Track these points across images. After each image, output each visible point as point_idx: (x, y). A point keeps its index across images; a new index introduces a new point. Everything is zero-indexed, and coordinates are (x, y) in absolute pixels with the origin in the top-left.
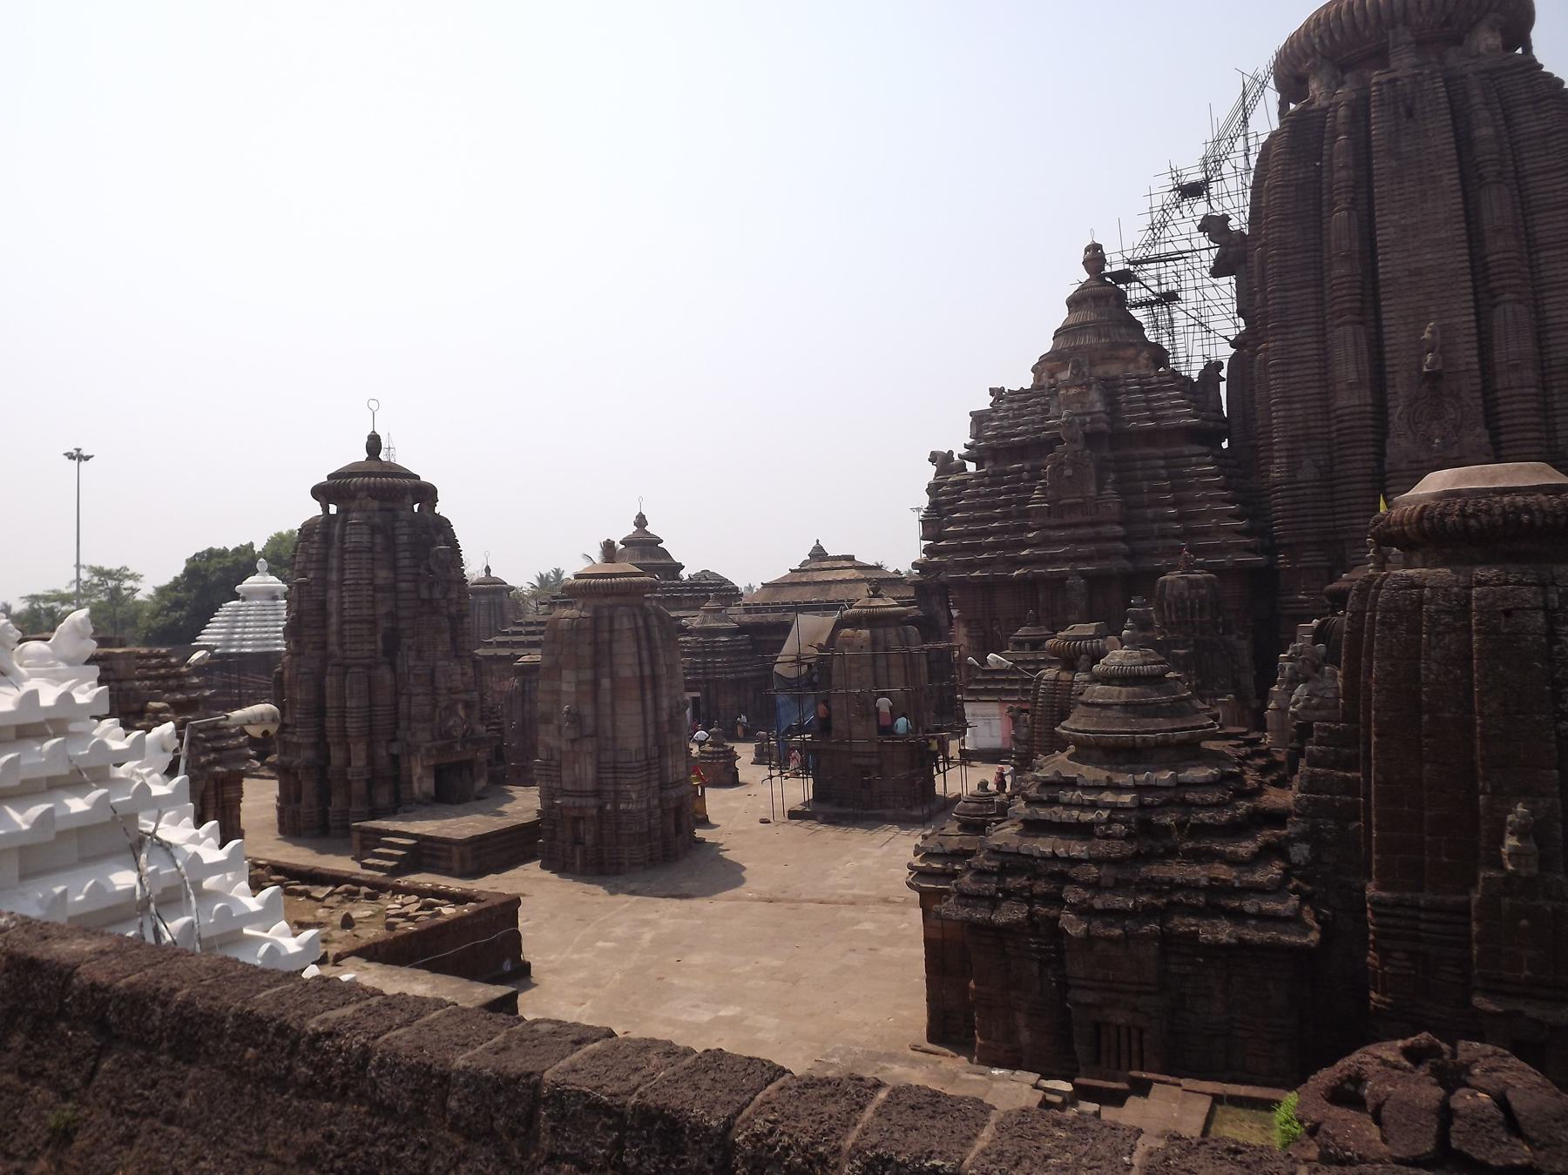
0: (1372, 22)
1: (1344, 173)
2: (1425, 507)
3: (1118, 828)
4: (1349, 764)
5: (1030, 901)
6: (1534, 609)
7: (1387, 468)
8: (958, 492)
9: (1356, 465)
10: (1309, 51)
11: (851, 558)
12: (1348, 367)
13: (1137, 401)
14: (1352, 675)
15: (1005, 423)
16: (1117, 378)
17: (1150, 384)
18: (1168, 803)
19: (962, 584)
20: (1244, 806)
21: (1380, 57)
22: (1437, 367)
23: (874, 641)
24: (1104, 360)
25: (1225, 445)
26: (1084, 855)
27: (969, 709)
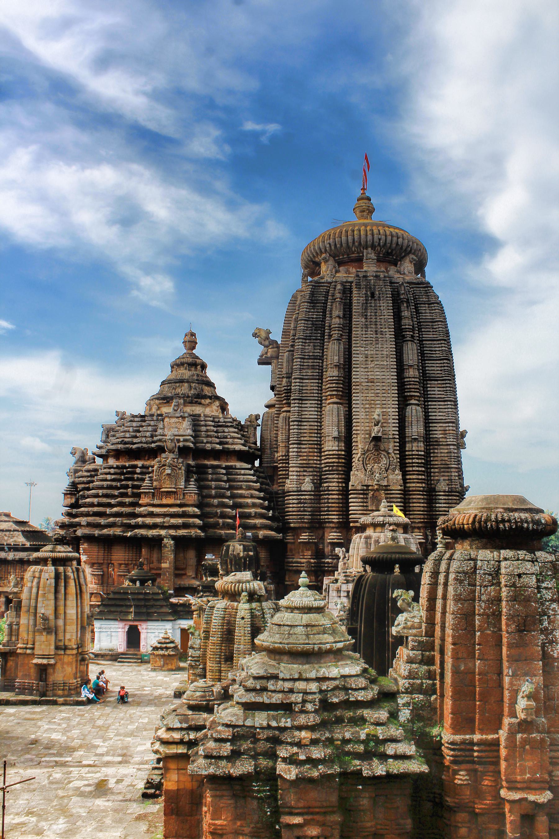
0: (356, 244)
1: (337, 320)
2: (476, 516)
3: (309, 707)
4: (430, 661)
5: (254, 757)
6: (533, 574)
7: (350, 488)
8: (91, 476)
9: (334, 484)
10: (323, 250)
11: (8, 515)
12: (332, 428)
13: (213, 431)
14: (431, 608)
15: (128, 435)
16: (199, 415)
17: (219, 422)
18: (336, 688)
19: (89, 539)
20: (376, 688)
21: (359, 261)
22: (380, 435)
23: (57, 576)
24: (191, 403)
25: (257, 463)
26: (289, 725)
27: (97, 624)
